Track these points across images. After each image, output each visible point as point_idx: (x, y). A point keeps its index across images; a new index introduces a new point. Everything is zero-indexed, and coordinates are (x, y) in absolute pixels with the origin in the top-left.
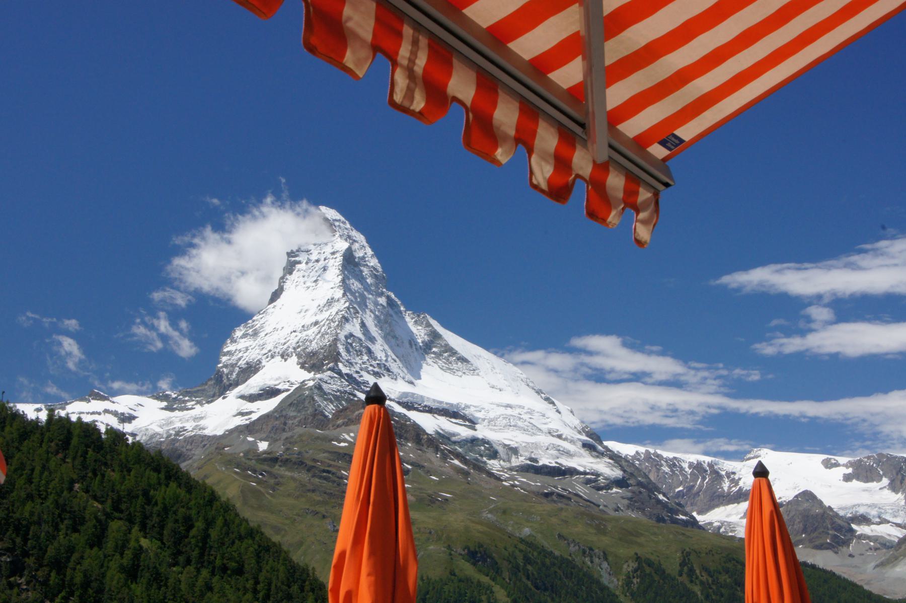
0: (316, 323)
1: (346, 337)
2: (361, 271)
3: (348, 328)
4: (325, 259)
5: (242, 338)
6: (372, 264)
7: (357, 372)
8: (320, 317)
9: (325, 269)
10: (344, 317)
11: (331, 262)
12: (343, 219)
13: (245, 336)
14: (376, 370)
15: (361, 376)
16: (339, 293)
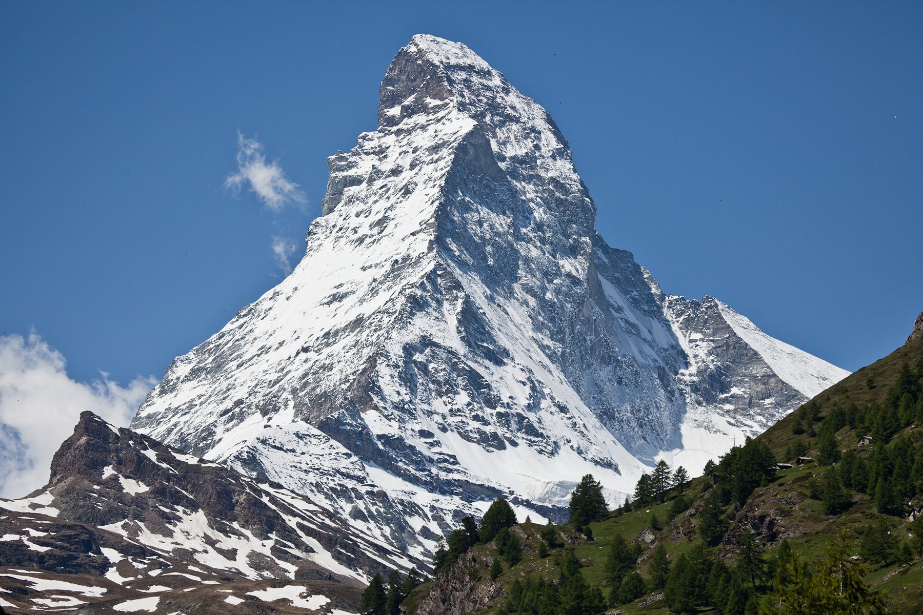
0: (358, 323)
1: (409, 349)
2: (514, 193)
3: (421, 324)
4: (412, 166)
5: (188, 379)
6: (550, 174)
7: (424, 434)
8: (367, 309)
9: (407, 191)
10: (412, 299)
11: (427, 169)
12: (485, 65)
13: (195, 373)
14: (488, 429)
15: (432, 445)
16: (421, 244)
